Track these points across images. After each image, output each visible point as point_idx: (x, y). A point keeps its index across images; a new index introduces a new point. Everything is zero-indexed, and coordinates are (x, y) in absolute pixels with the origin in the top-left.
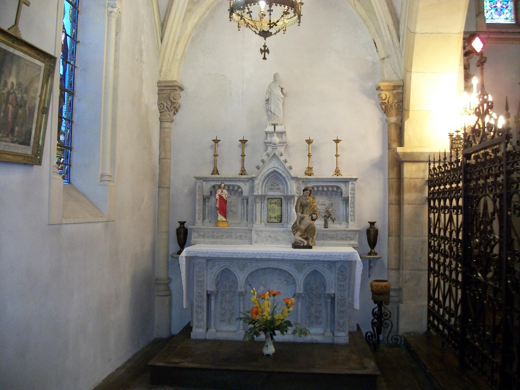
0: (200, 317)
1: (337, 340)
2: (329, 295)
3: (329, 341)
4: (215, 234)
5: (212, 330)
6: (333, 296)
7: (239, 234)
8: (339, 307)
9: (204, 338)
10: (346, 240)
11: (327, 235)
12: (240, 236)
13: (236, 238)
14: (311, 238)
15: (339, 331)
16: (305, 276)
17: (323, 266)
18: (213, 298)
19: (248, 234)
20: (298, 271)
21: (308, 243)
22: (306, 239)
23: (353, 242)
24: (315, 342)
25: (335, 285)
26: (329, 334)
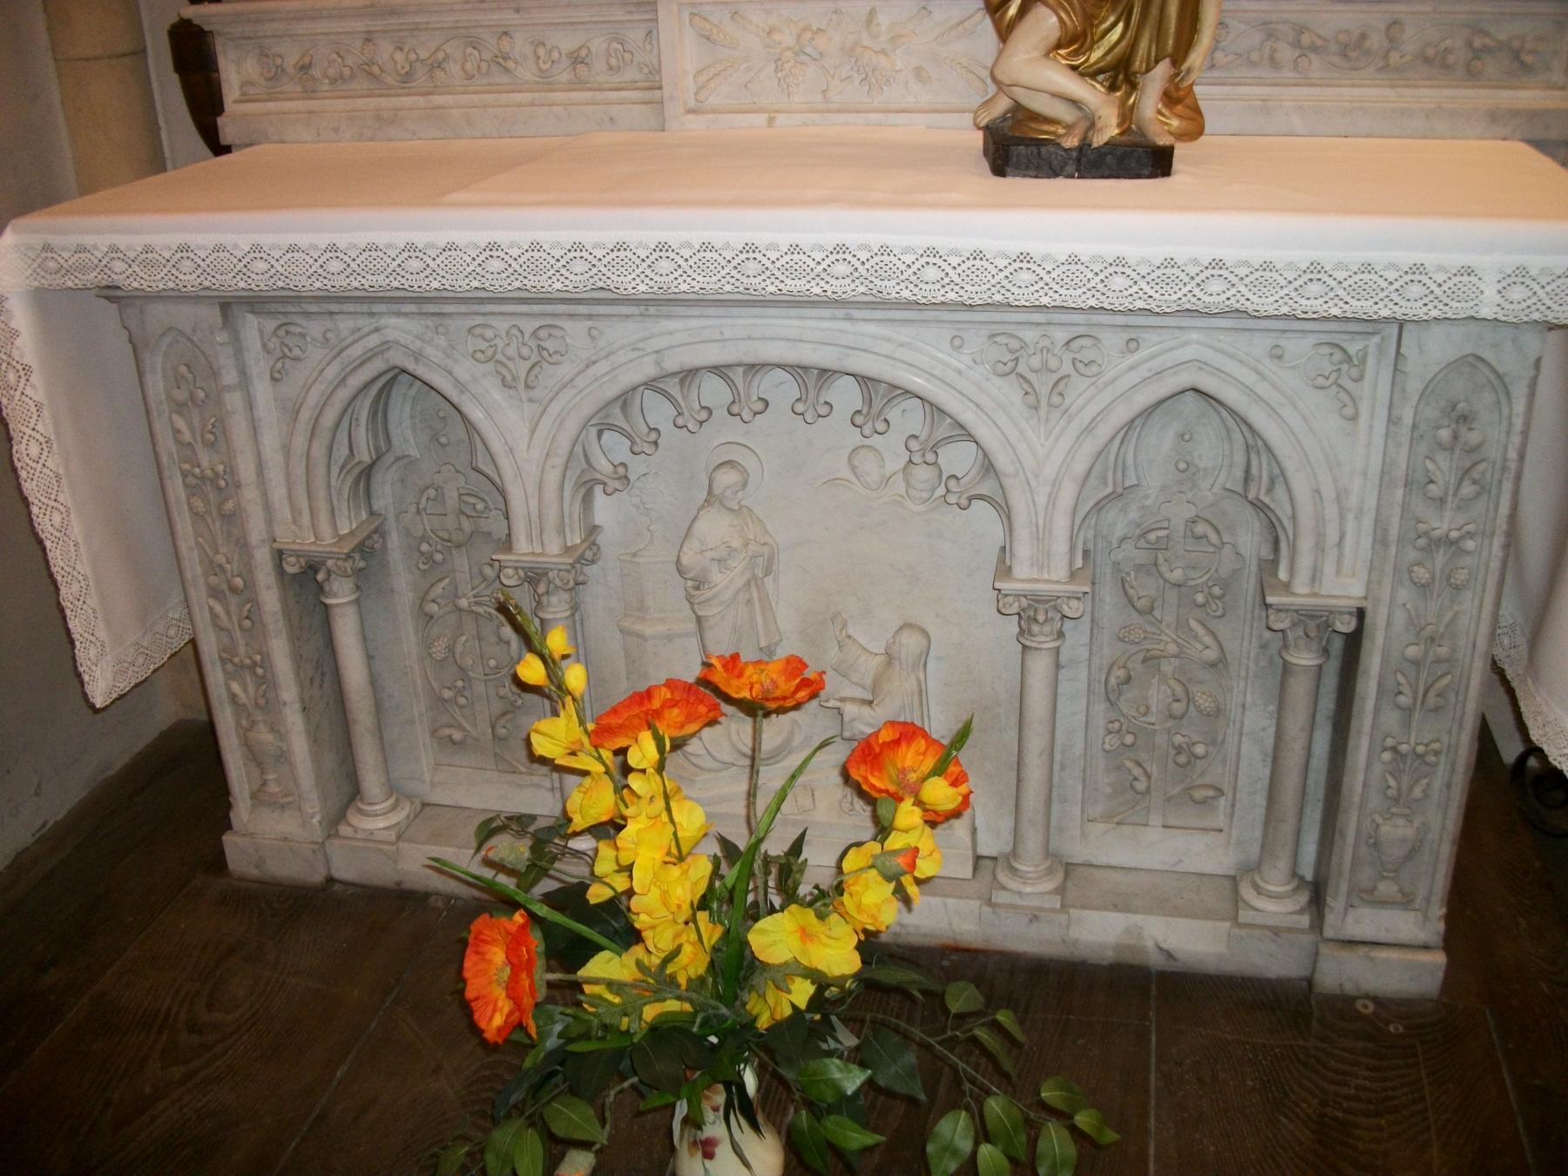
0: (264, 735)
1: (1342, 973)
2: (1316, 621)
3: (1275, 961)
4: (384, 51)
5: (377, 820)
6: (1346, 625)
7: (567, 42)
8: (1391, 719)
9: (318, 877)
10: (1472, 75)
11: (1300, 29)
12: (577, 59)
13: (546, 83)
14: (1162, 70)
15: (1367, 896)
16: (1090, 447)
17: (1278, 356)
18: (341, 595)
19: (635, 36)
20: (1029, 390)
21: (1127, 115)
22: (1120, 74)
23: (1529, 97)
24: (1156, 961)
25: (1381, 540)
26: (1276, 904)
